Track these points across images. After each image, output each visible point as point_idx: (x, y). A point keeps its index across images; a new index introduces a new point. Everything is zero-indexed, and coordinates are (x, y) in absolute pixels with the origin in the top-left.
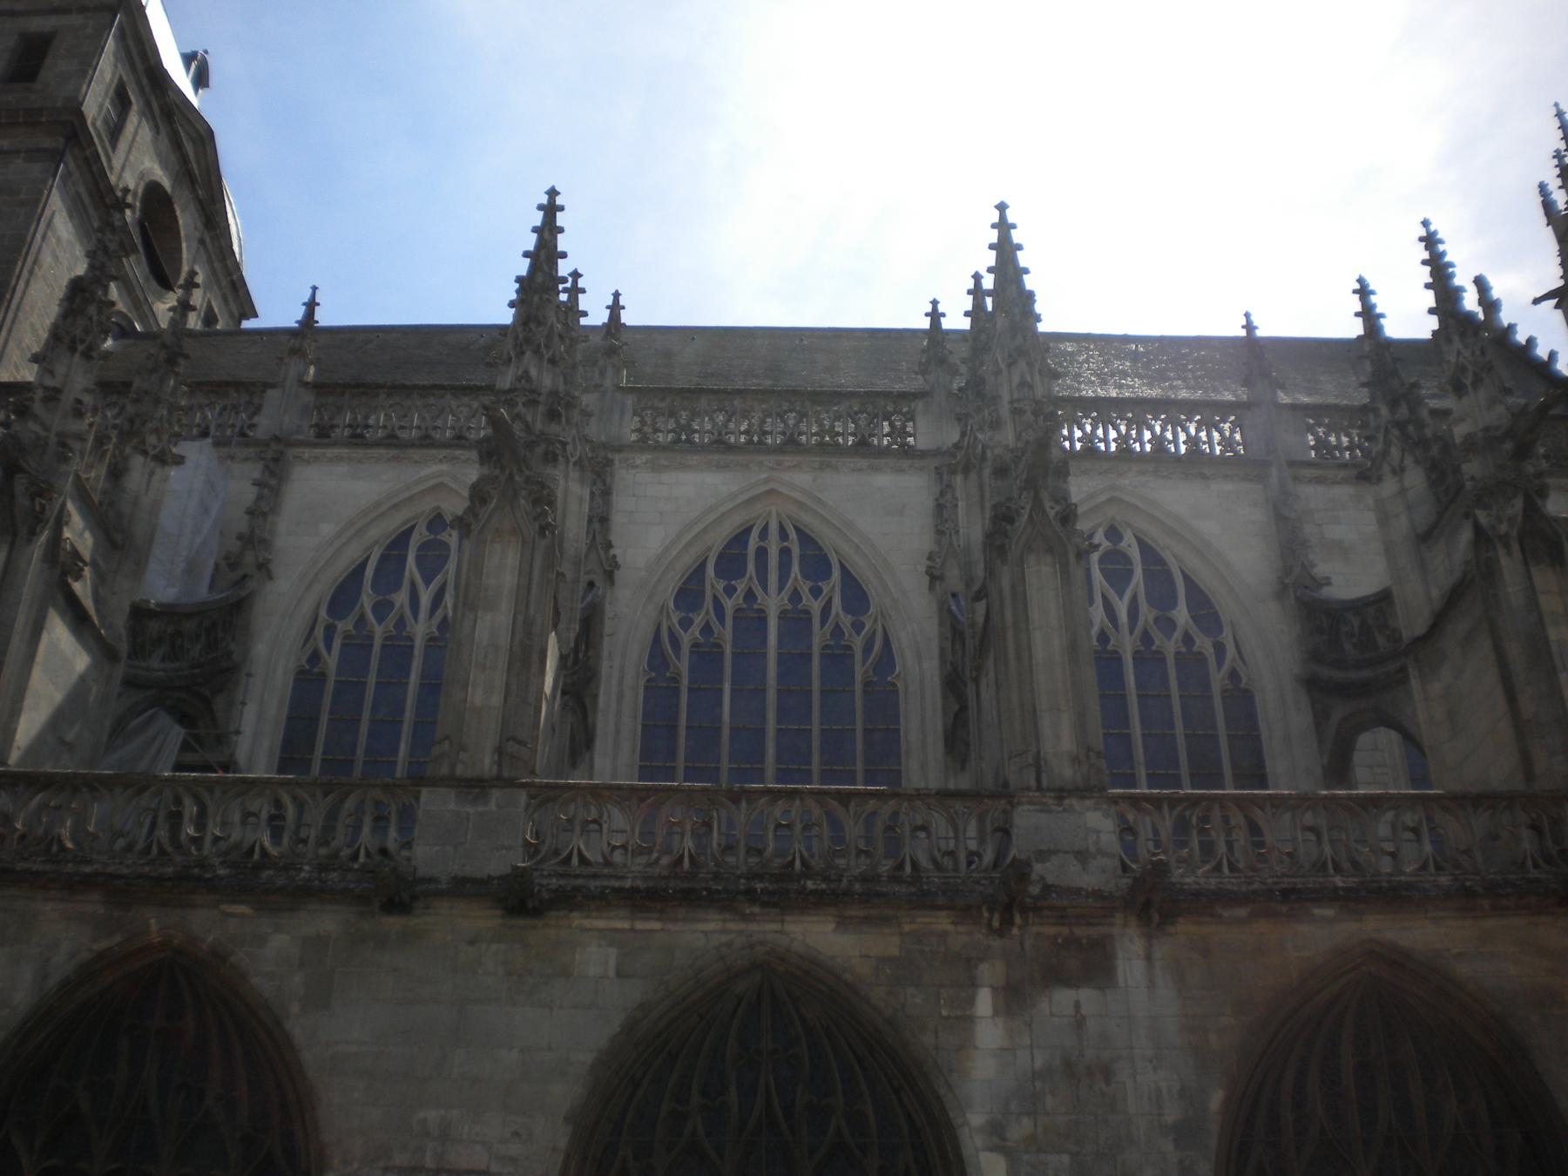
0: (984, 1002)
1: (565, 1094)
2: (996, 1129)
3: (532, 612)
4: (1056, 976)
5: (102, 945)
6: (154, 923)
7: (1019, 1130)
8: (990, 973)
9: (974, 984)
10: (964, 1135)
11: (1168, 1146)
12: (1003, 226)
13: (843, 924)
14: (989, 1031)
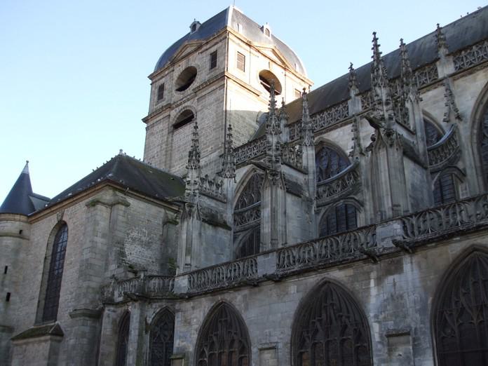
0: (372, 283)
1: (289, 322)
2: (376, 316)
3: (274, 205)
4: (389, 272)
5: (212, 305)
6: (219, 298)
7: (381, 317)
8: (373, 275)
9: (370, 279)
10: (369, 318)
11: (418, 316)
12: (375, 40)
13: (340, 269)
14: (374, 291)
